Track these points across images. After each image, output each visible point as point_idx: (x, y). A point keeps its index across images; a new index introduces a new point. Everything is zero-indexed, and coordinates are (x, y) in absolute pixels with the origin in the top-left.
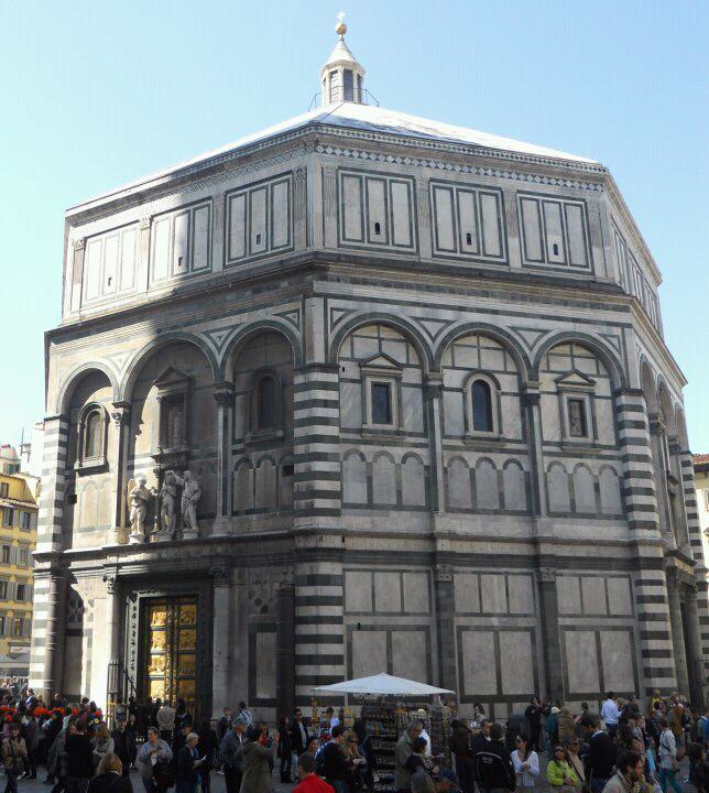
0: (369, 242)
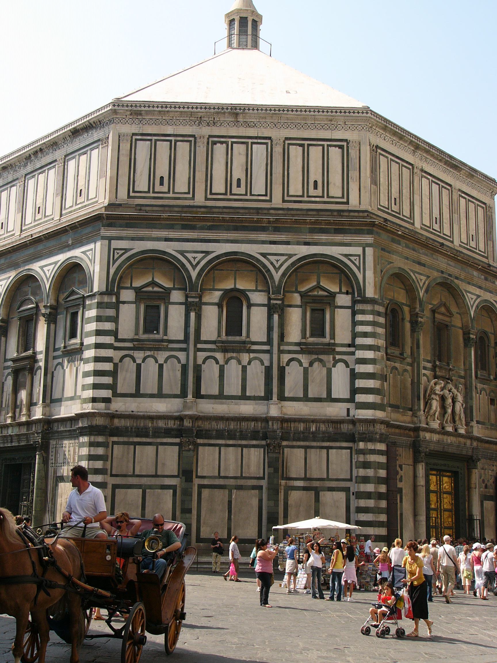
0: (154, 192)
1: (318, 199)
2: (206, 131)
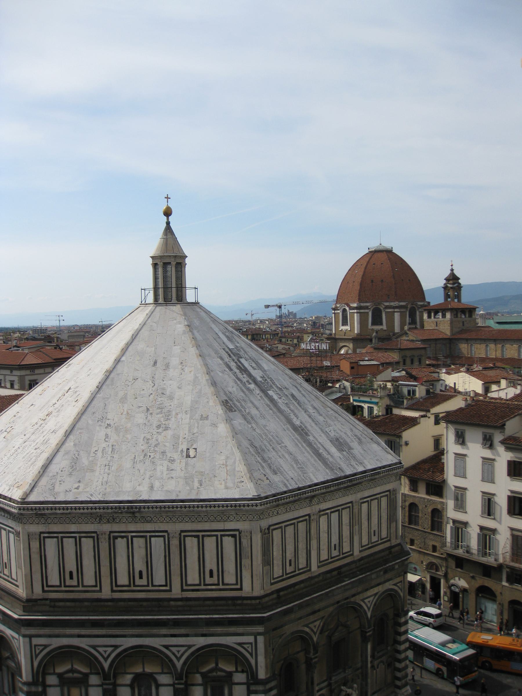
0: (65, 586)
1: (214, 587)
2: (107, 528)
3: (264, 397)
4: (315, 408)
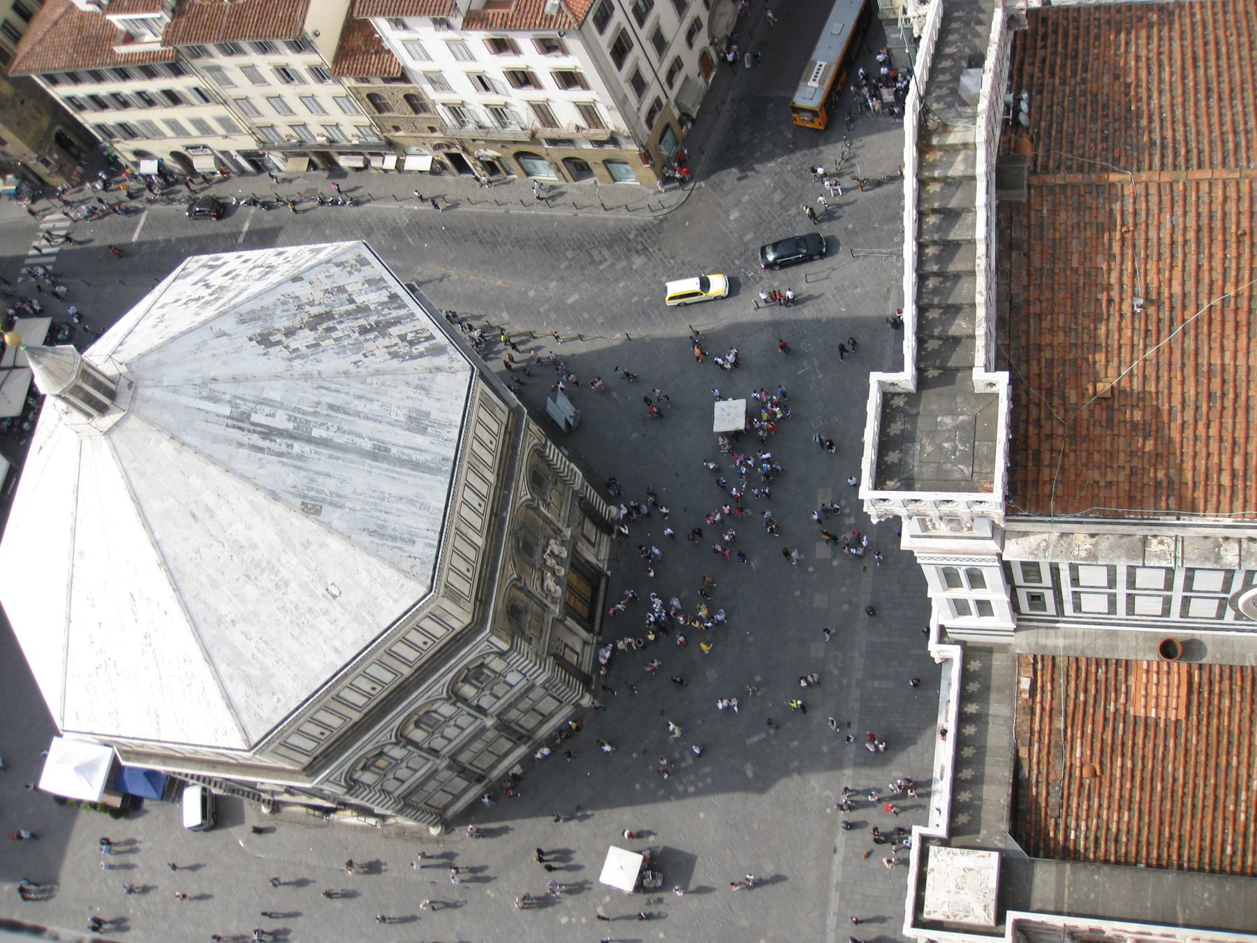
3: (318, 450)
4: (360, 397)
